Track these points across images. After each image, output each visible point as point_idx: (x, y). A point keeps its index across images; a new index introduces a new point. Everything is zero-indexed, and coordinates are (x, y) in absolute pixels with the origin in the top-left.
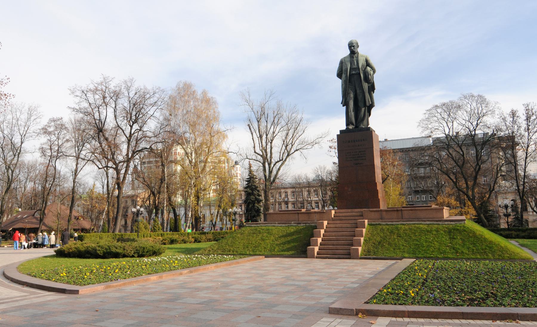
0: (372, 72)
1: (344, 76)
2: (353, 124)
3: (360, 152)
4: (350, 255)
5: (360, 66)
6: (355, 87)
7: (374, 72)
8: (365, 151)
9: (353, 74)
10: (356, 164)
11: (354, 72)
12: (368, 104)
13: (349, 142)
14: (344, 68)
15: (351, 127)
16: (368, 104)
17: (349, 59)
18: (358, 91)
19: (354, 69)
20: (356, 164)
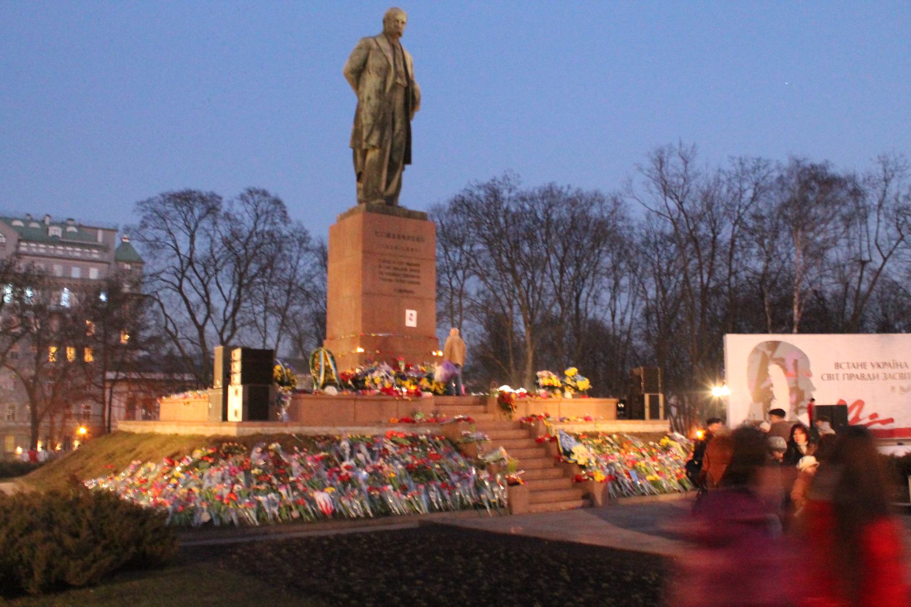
3: (409, 264)
8: (418, 265)
10: (401, 291)
13: (388, 236)
14: (373, 62)
20: (401, 291)
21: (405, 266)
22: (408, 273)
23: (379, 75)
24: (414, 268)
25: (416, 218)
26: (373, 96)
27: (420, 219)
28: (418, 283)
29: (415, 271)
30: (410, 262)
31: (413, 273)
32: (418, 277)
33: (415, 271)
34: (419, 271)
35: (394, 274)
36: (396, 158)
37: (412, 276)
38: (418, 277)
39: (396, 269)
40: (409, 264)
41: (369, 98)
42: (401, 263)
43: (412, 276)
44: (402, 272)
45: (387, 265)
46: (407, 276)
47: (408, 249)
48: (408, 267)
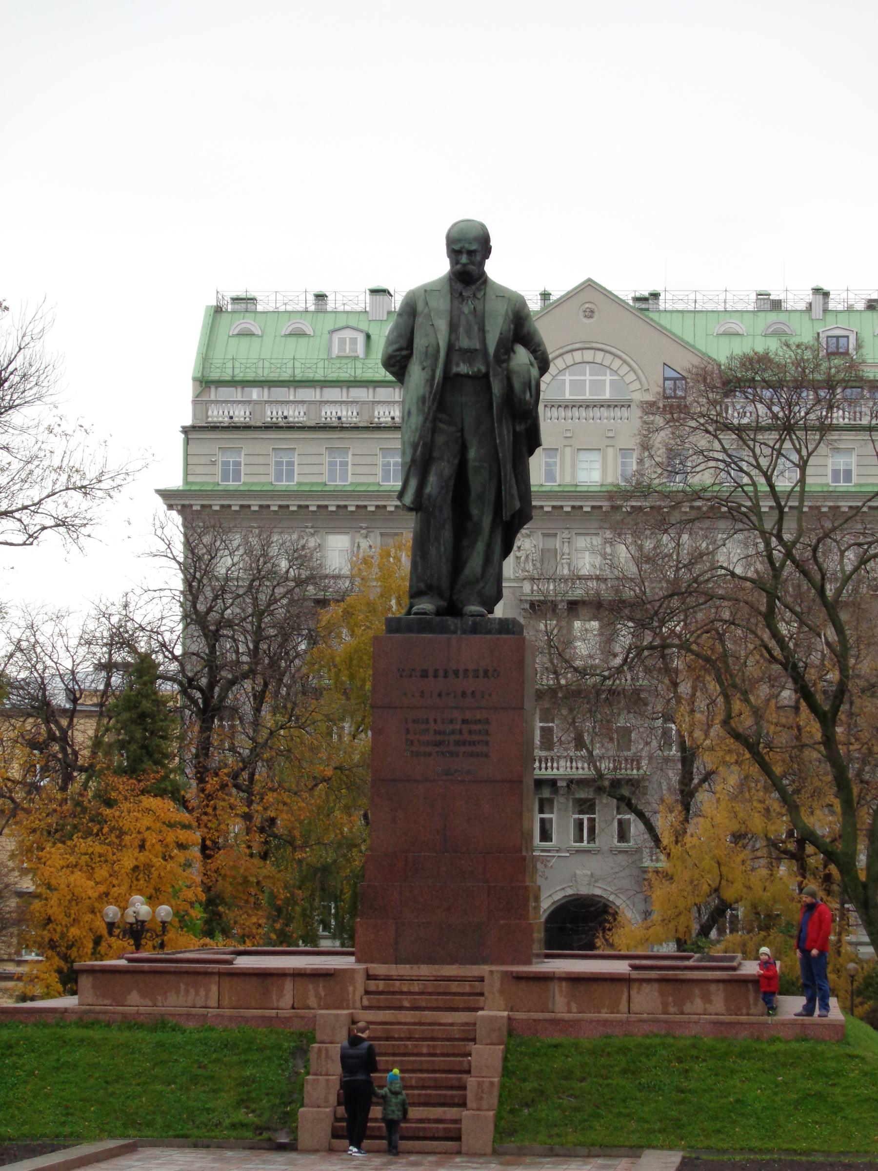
0: (535, 372)
1: (416, 373)
2: (440, 595)
3: (464, 721)
4: (458, 1139)
5: (491, 350)
6: (462, 430)
7: (544, 365)
8: (487, 722)
9: (458, 375)
11: (463, 368)
12: (506, 514)
13: (424, 674)
14: (420, 343)
15: (426, 605)
16: (506, 514)
17: (442, 304)
18: (472, 454)
19: (469, 354)
21: (458, 727)
22: (466, 736)
23: (423, 369)
24: (477, 727)
25: (489, 632)
26: (414, 410)
27: (500, 633)
28: (487, 756)
29: (480, 732)
30: (468, 715)
31: (475, 738)
32: (487, 743)
33: (480, 732)
34: (487, 733)
35: (439, 744)
36: (475, 511)
37: (473, 743)
38: (487, 743)
39: (440, 733)
40: (464, 721)
41: (409, 413)
42: (451, 721)
43: (473, 743)
44: (452, 738)
45: (423, 727)
46: (464, 744)
47: (464, 694)
48: (465, 728)
